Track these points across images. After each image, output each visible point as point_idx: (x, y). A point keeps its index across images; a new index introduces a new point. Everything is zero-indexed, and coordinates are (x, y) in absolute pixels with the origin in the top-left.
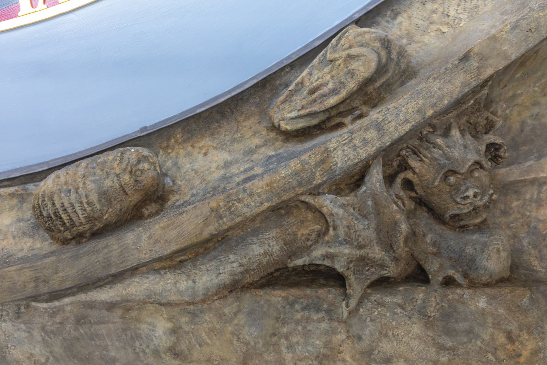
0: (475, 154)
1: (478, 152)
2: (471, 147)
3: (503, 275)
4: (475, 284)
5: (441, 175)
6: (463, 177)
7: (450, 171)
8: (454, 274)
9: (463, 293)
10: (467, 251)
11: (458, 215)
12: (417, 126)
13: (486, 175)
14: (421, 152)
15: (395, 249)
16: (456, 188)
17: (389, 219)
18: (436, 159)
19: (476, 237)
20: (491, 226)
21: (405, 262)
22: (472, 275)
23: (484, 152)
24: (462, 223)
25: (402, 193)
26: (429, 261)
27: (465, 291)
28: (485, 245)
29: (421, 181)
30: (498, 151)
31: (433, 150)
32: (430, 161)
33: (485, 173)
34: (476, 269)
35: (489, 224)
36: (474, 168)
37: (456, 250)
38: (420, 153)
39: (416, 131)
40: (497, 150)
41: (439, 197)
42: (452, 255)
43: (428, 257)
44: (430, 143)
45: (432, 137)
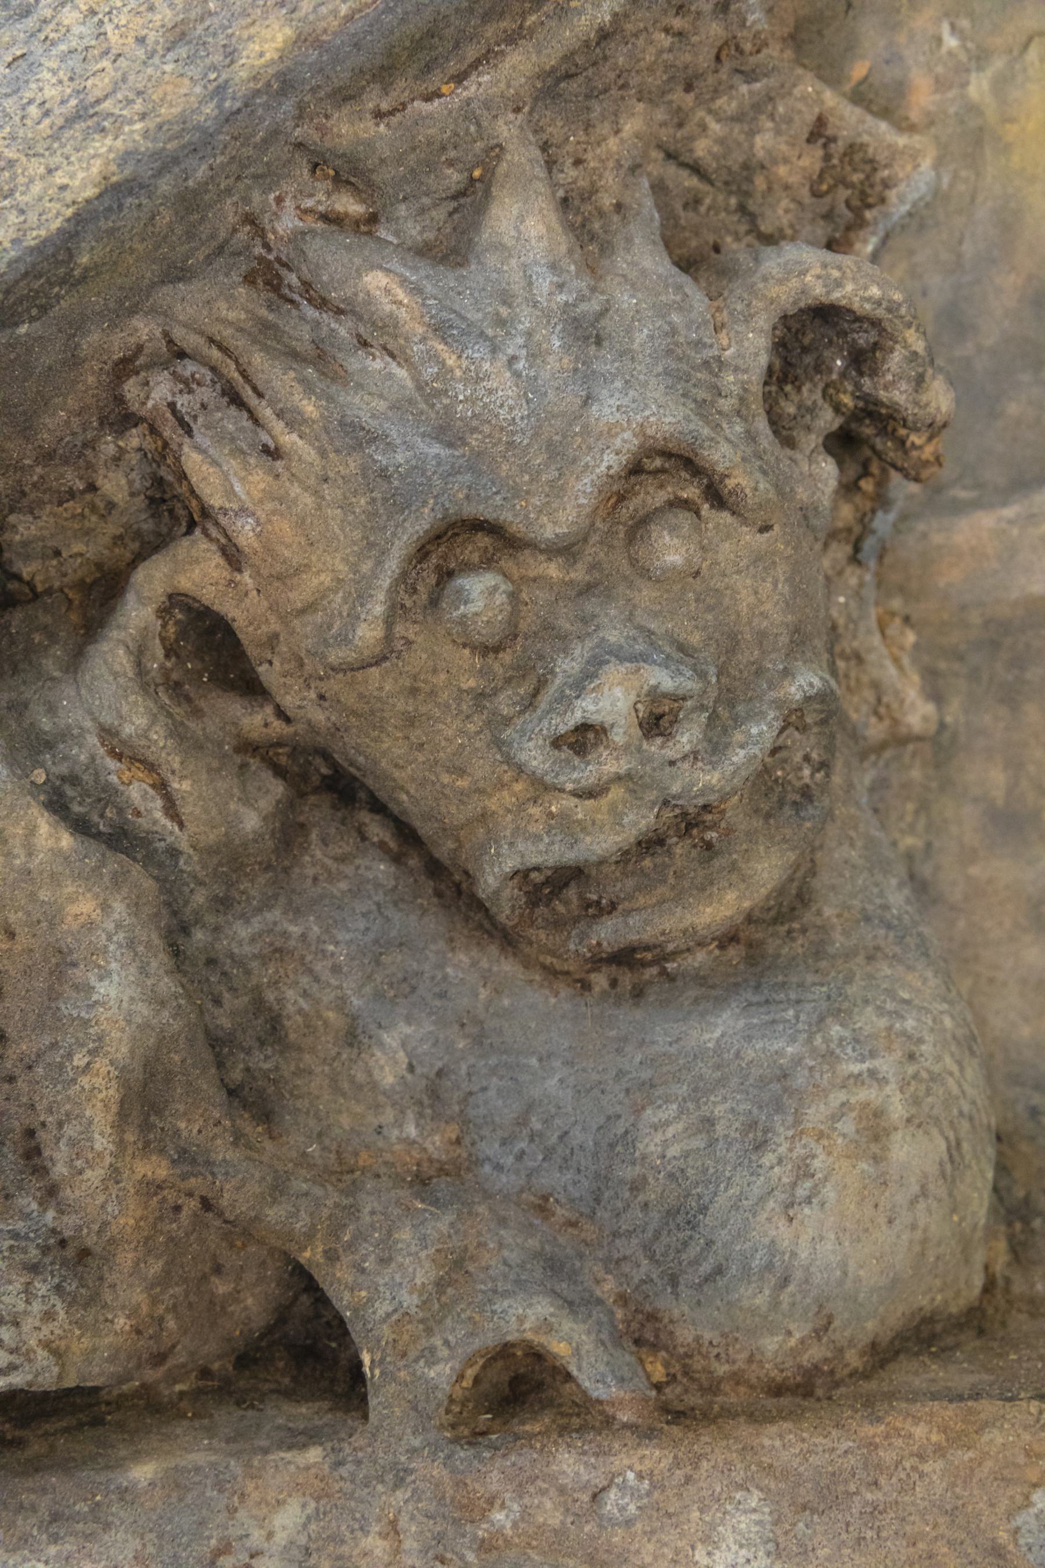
0: (656, 391)
1: (691, 372)
2: (641, 336)
3: (923, 1301)
4: (713, 1388)
5: (393, 565)
6: (579, 574)
7: (478, 526)
8: (546, 1326)
9: (601, 1482)
10: (650, 1144)
11: (569, 875)
12: (166, 163)
13: (758, 559)
14: (259, 380)
15: (60, 1170)
16: (518, 658)
17: (11, 935)
18: (356, 436)
19: (721, 1028)
20: (839, 941)
21: (155, 1267)
22: (691, 1324)
23: (755, 377)
24: (607, 933)
25: (136, 719)
26: (360, 1236)
27: (619, 1462)
28: (779, 1091)
29: (284, 619)
30: (874, 373)
31: (356, 362)
32: (323, 453)
33: (749, 537)
34: (707, 1279)
35: (824, 929)
36: (661, 497)
37: (577, 1136)
38: (260, 395)
39: (190, 203)
40: (862, 360)
41: (417, 735)
42: (552, 1179)
43: (353, 1211)
44: (323, 304)
45: (331, 260)
